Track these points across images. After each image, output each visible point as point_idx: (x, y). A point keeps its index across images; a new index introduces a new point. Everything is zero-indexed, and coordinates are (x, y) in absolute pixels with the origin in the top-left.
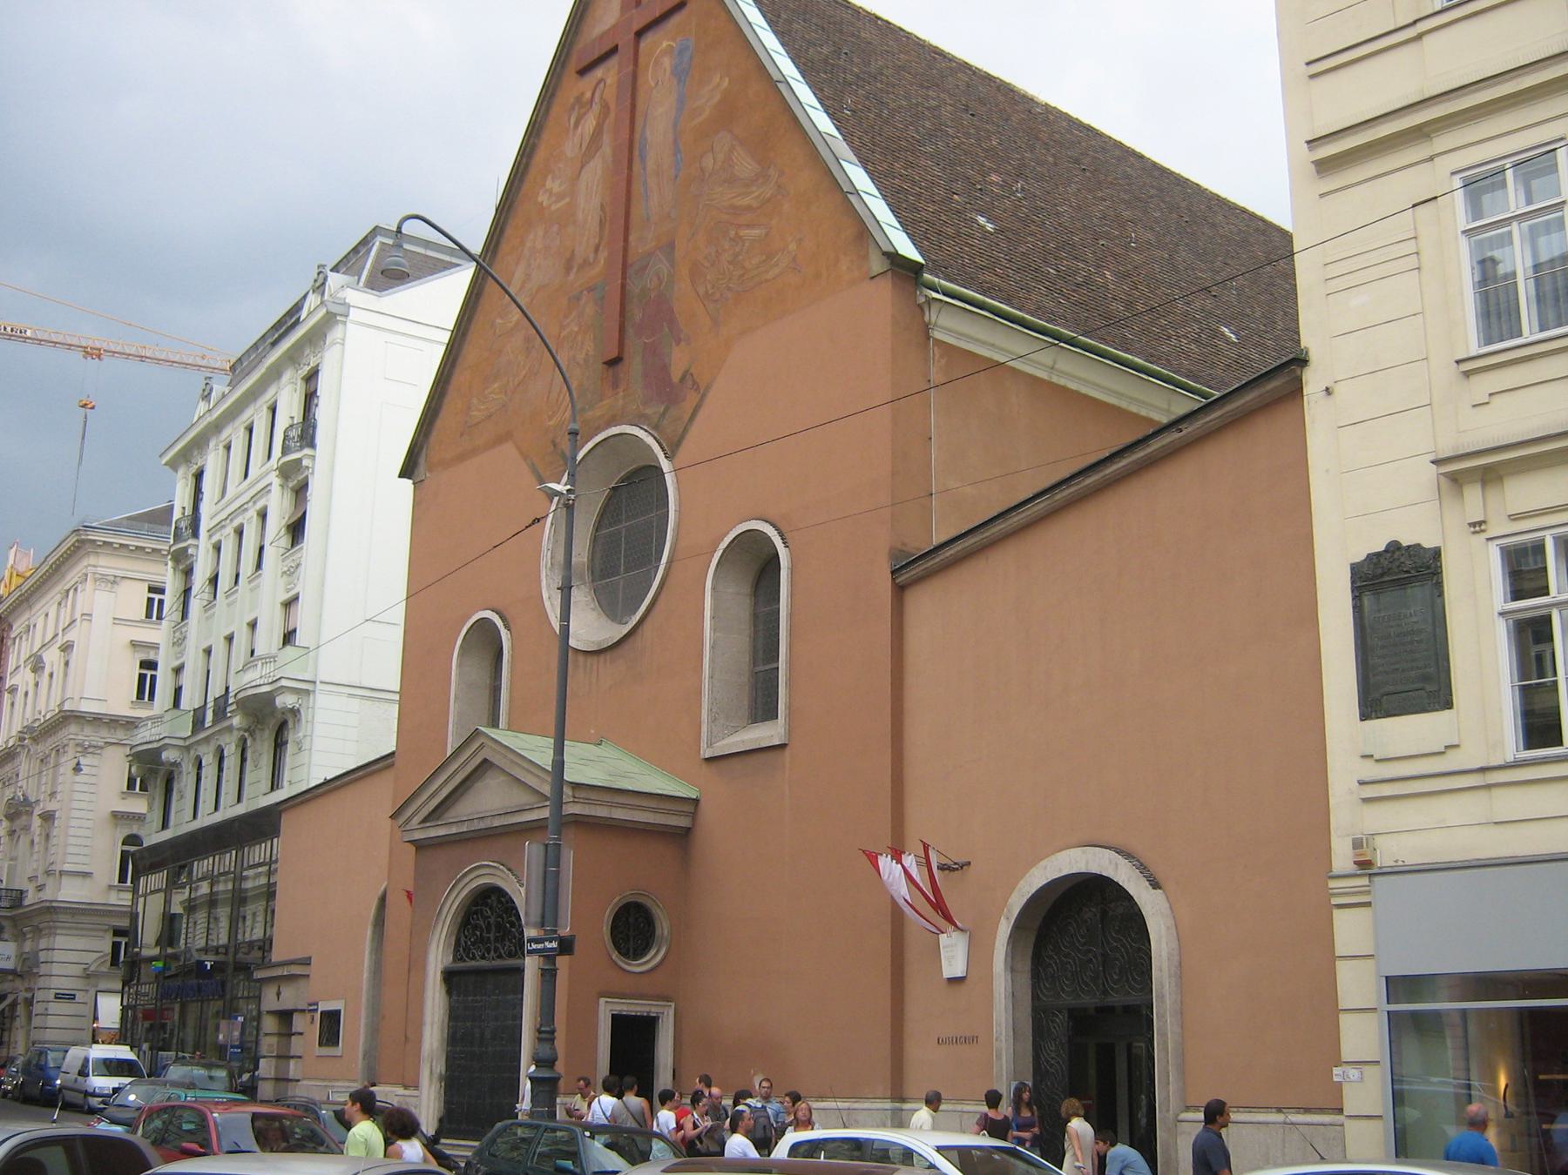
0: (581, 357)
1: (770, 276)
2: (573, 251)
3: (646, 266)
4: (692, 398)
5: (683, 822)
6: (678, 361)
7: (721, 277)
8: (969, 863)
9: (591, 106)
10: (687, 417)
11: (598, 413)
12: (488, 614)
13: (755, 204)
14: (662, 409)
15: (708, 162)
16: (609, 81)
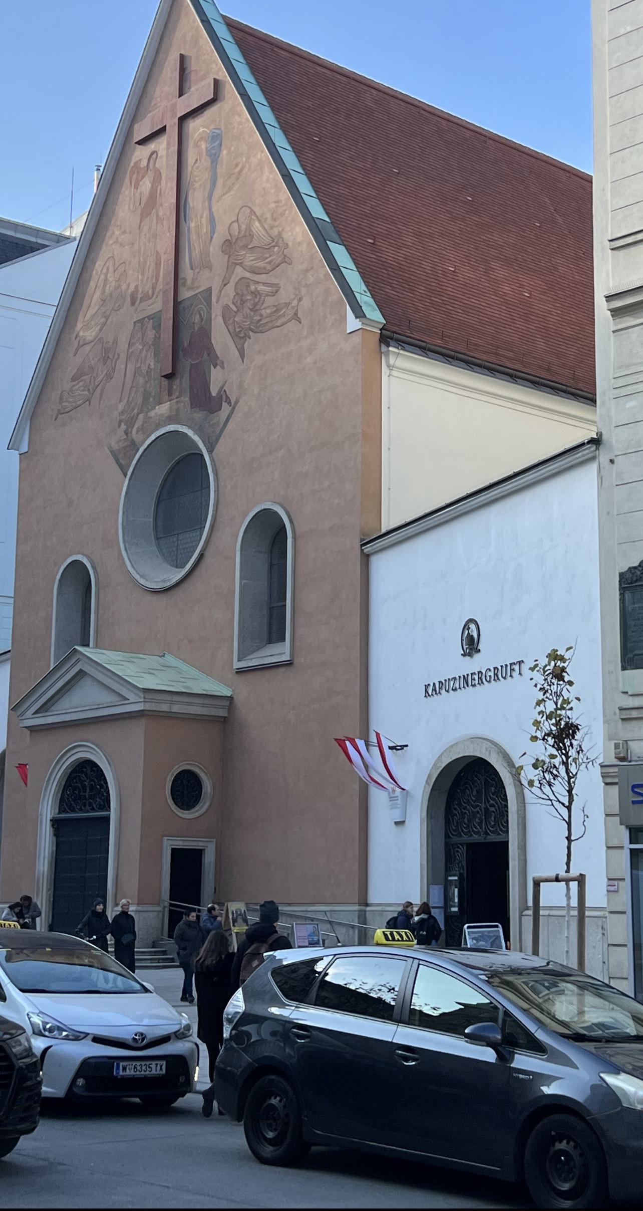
0: (144, 369)
4: (226, 409)
5: (223, 713)
7: (244, 320)
8: (407, 746)
12: (79, 557)
13: (269, 267)
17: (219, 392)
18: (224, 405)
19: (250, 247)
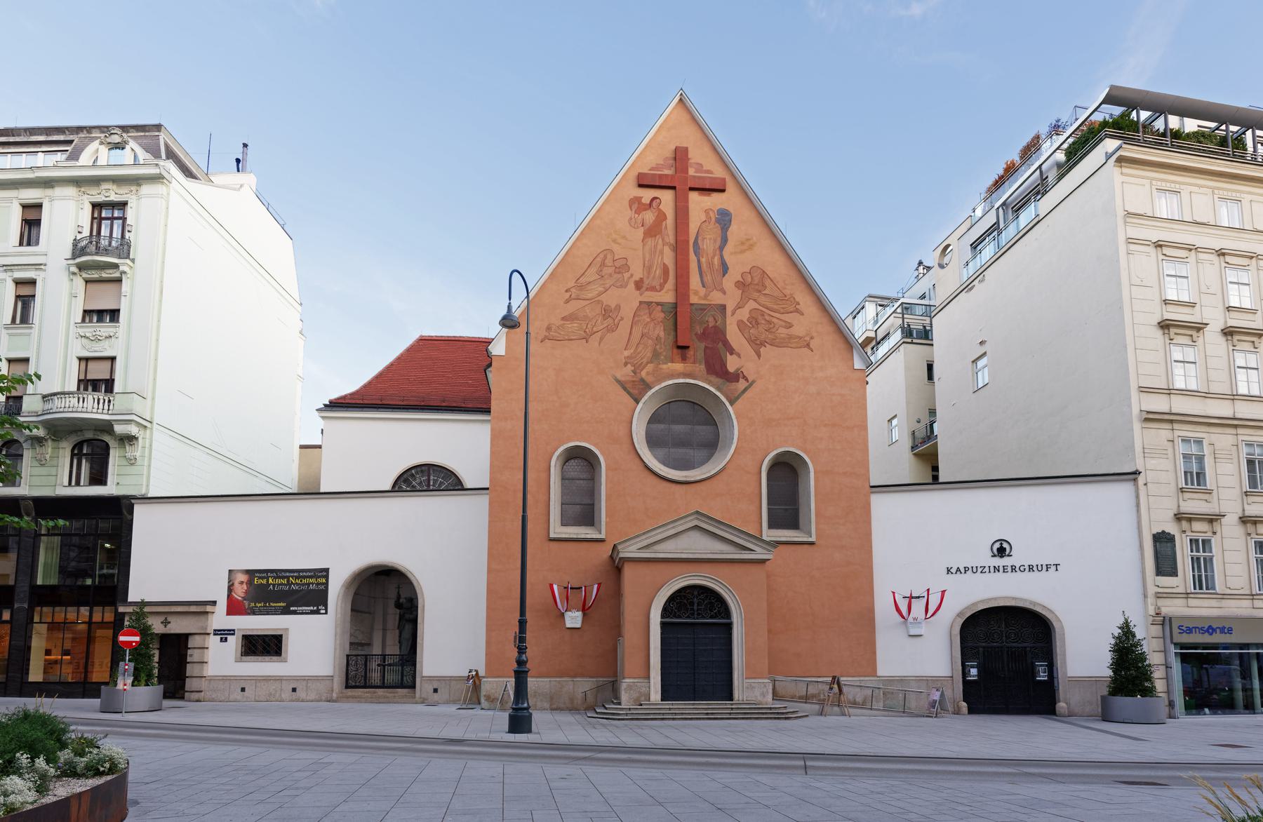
3: (705, 310)
4: (742, 384)
6: (732, 364)
17: (738, 369)
18: (742, 381)
19: (764, 292)
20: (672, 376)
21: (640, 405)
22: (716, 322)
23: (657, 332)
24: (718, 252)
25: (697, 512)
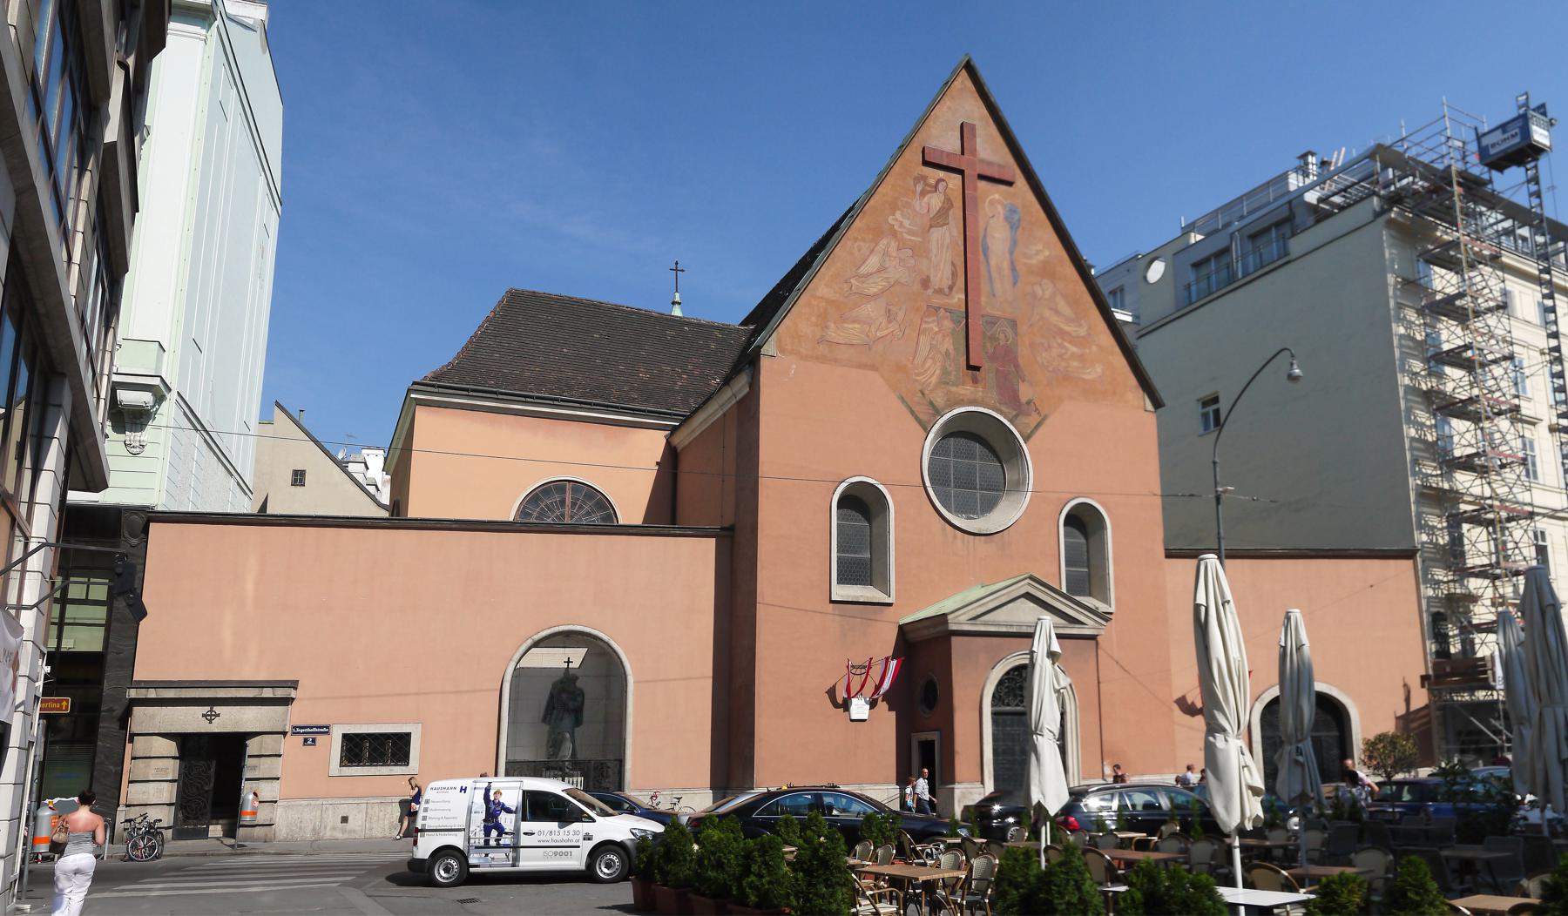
0: (943, 350)
1: (1087, 377)
2: (928, 277)
3: (995, 324)
6: (1025, 392)
9: (936, 190)
10: (1033, 425)
11: (962, 392)
13: (1074, 334)
14: (1014, 413)
15: (1040, 292)
16: (950, 186)
20: (961, 403)
21: (931, 436)
22: (1007, 341)
23: (946, 346)
24: (1008, 256)
25: (1031, 578)
